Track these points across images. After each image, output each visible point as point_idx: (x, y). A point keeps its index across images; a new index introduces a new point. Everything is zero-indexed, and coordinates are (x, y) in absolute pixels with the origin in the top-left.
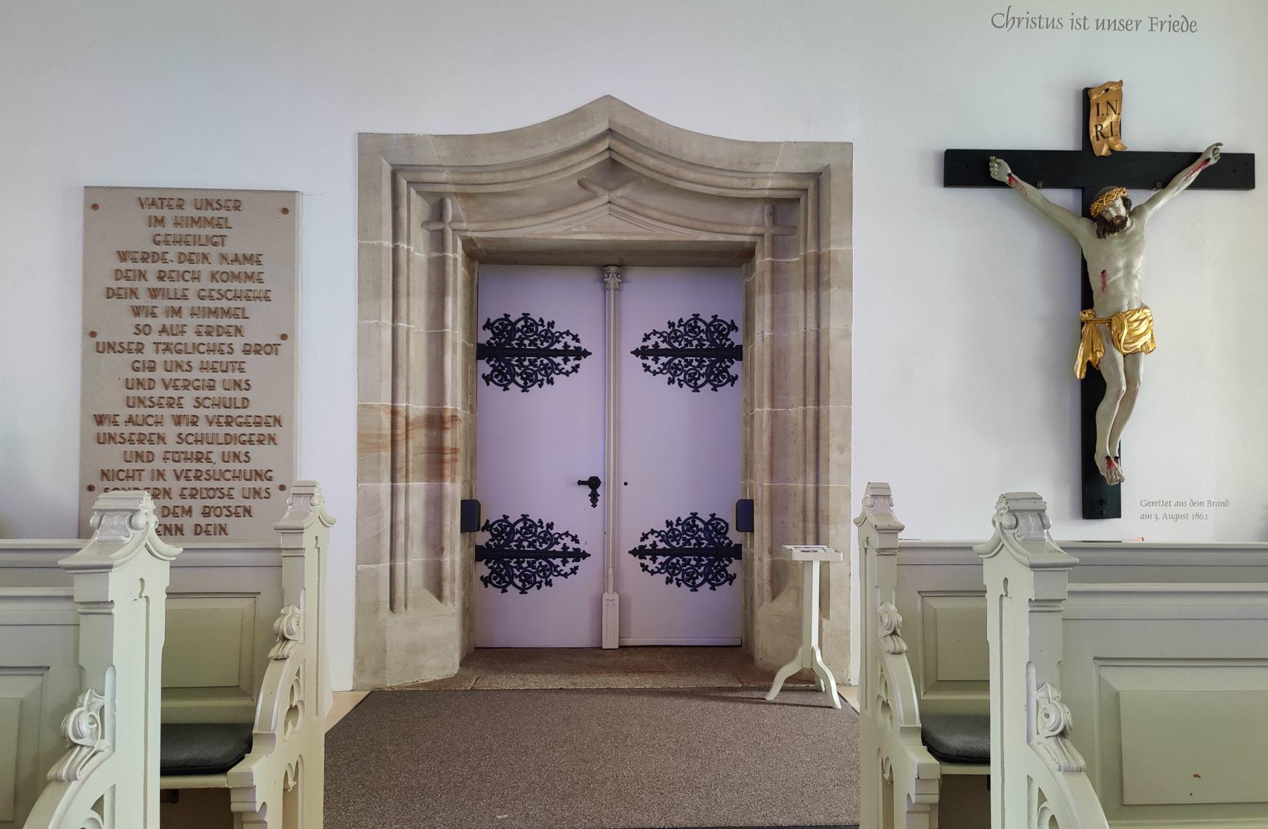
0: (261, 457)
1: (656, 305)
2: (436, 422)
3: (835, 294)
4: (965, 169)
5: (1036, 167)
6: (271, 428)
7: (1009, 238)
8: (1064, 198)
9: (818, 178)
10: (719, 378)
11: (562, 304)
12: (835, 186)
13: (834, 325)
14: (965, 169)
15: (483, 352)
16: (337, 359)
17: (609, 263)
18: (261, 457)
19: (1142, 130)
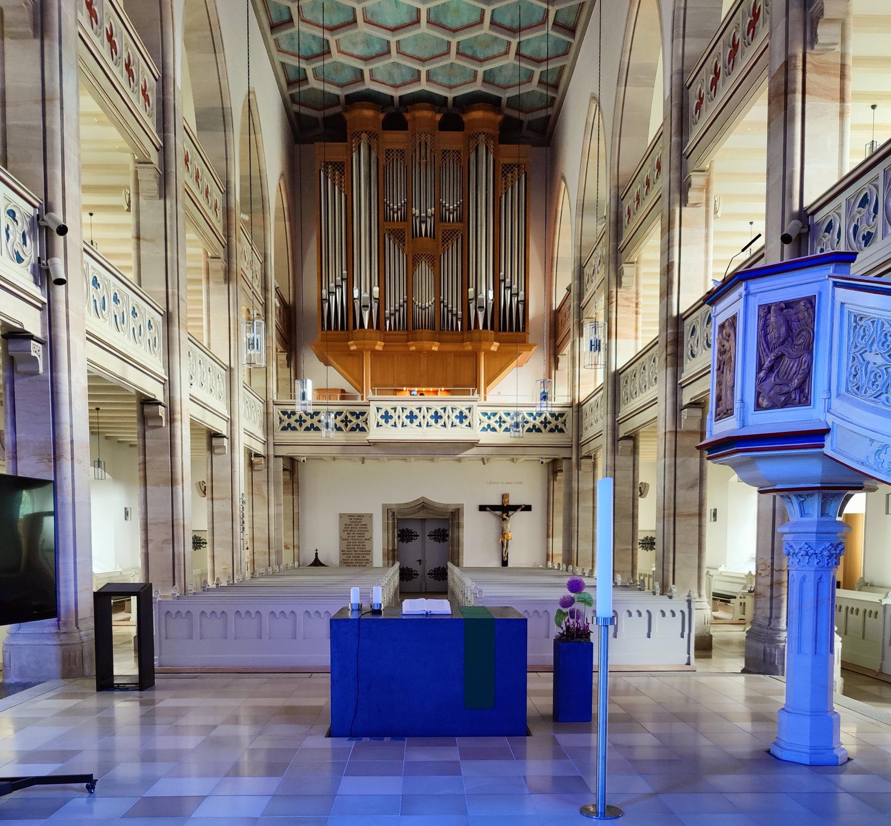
0: (367, 557)
1: (431, 528)
2: (394, 550)
3: (461, 530)
4: (482, 508)
5: (493, 508)
6: (369, 552)
7: (489, 518)
8: (499, 513)
9: (458, 509)
10: (444, 540)
11: (415, 528)
12: (461, 511)
13: (461, 534)
14: (482, 508)
15: (398, 536)
16: (378, 540)
17: (423, 520)
18: (367, 557)
19: (512, 502)
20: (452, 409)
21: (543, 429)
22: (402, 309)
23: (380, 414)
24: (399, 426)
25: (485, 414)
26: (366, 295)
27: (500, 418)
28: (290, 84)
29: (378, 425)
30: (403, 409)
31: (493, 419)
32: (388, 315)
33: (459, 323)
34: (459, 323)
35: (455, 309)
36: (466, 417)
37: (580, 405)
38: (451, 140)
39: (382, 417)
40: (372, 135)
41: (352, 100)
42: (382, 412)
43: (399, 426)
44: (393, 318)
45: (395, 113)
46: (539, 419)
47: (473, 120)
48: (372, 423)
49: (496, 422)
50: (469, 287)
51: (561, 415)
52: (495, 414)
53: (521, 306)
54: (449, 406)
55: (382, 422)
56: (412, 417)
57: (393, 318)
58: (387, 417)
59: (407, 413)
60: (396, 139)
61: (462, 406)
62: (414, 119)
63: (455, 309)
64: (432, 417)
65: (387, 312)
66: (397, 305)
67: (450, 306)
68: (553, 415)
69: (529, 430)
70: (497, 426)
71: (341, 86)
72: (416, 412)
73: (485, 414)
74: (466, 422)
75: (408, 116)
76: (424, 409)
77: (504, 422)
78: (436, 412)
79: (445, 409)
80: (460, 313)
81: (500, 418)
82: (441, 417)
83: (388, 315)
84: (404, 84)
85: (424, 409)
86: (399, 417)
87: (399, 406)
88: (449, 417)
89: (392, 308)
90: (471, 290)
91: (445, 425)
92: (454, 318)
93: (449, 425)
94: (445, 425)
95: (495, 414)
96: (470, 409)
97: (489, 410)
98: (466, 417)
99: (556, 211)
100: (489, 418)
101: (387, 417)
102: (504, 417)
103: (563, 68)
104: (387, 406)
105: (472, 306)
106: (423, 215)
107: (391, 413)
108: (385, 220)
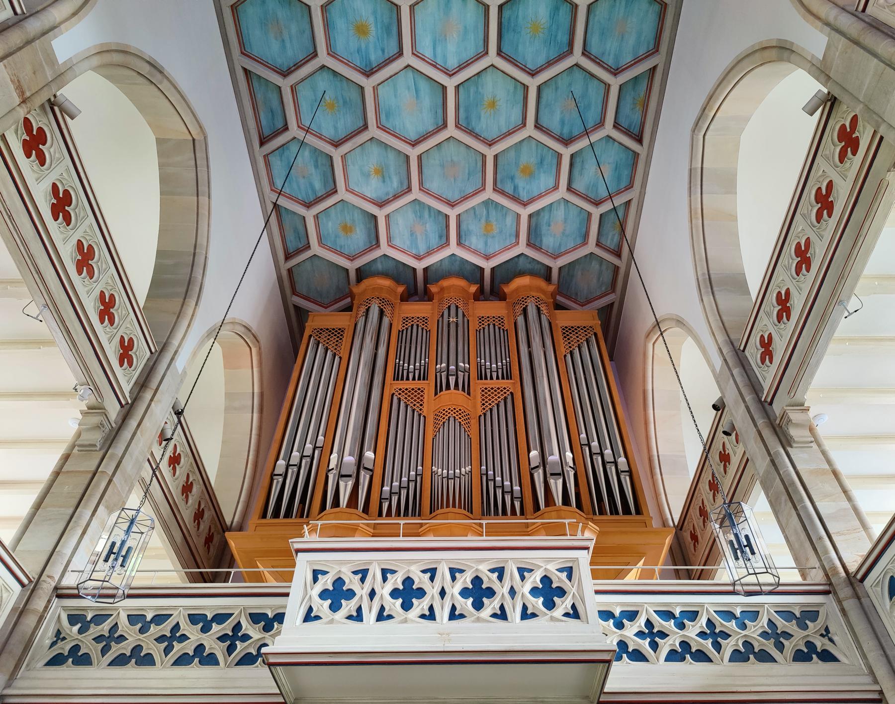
20: (521, 571)
21: (775, 653)
22: (412, 485)
23: (319, 588)
24: (370, 616)
25: (606, 615)
26: (349, 459)
27: (649, 624)
28: (288, 257)
29: (309, 617)
30: (385, 572)
31: (630, 630)
32: (386, 495)
33: (517, 504)
34: (517, 504)
35: (507, 483)
36: (561, 592)
37: (855, 581)
38: (492, 309)
39: (324, 595)
40: (382, 300)
41: (361, 274)
42: (326, 582)
43: (370, 616)
44: (395, 499)
45: (416, 287)
46: (754, 631)
47: (517, 290)
48: (294, 610)
49: (640, 634)
50: (529, 451)
51: (811, 615)
52: (632, 615)
53: (626, 480)
54: (512, 560)
55: (322, 607)
56: (408, 593)
57: (395, 499)
58: (337, 594)
59: (395, 581)
60: (417, 309)
61: (549, 560)
62: (442, 289)
63: (507, 483)
64: (465, 593)
65: (386, 488)
66: (405, 479)
67: (498, 479)
68: (787, 615)
69: (738, 656)
70: (644, 645)
71: (352, 258)
72: (421, 580)
73: (606, 615)
74: (563, 605)
75: (433, 289)
76: (443, 572)
77: (663, 635)
78: (477, 580)
79: (500, 572)
80: (517, 488)
81: (649, 624)
82: (491, 593)
83: (386, 495)
84: (429, 253)
85: (443, 572)
86: (372, 594)
87: (375, 562)
88: (512, 592)
89: (396, 484)
90: (534, 453)
91: (502, 615)
92: (508, 498)
93: (515, 614)
94: (502, 615)
95: (632, 615)
96: (569, 572)
97: (617, 604)
98: (561, 592)
99: (645, 392)
100: (620, 626)
101: (337, 594)
102: (659, 623)
103: (628, 203)
104: (341, 566)
105: (539, 476)
106: (452, 367)
107: (352, 582)
108: (396, 377)
